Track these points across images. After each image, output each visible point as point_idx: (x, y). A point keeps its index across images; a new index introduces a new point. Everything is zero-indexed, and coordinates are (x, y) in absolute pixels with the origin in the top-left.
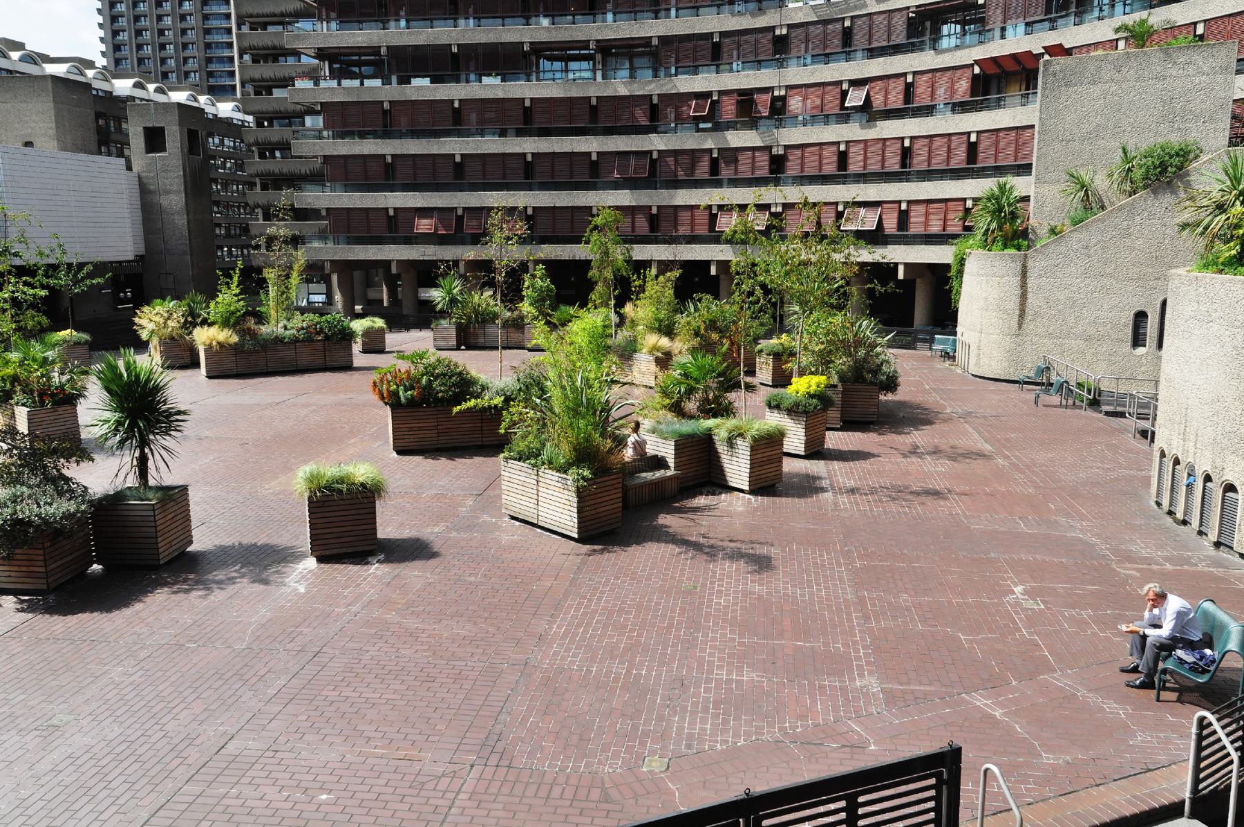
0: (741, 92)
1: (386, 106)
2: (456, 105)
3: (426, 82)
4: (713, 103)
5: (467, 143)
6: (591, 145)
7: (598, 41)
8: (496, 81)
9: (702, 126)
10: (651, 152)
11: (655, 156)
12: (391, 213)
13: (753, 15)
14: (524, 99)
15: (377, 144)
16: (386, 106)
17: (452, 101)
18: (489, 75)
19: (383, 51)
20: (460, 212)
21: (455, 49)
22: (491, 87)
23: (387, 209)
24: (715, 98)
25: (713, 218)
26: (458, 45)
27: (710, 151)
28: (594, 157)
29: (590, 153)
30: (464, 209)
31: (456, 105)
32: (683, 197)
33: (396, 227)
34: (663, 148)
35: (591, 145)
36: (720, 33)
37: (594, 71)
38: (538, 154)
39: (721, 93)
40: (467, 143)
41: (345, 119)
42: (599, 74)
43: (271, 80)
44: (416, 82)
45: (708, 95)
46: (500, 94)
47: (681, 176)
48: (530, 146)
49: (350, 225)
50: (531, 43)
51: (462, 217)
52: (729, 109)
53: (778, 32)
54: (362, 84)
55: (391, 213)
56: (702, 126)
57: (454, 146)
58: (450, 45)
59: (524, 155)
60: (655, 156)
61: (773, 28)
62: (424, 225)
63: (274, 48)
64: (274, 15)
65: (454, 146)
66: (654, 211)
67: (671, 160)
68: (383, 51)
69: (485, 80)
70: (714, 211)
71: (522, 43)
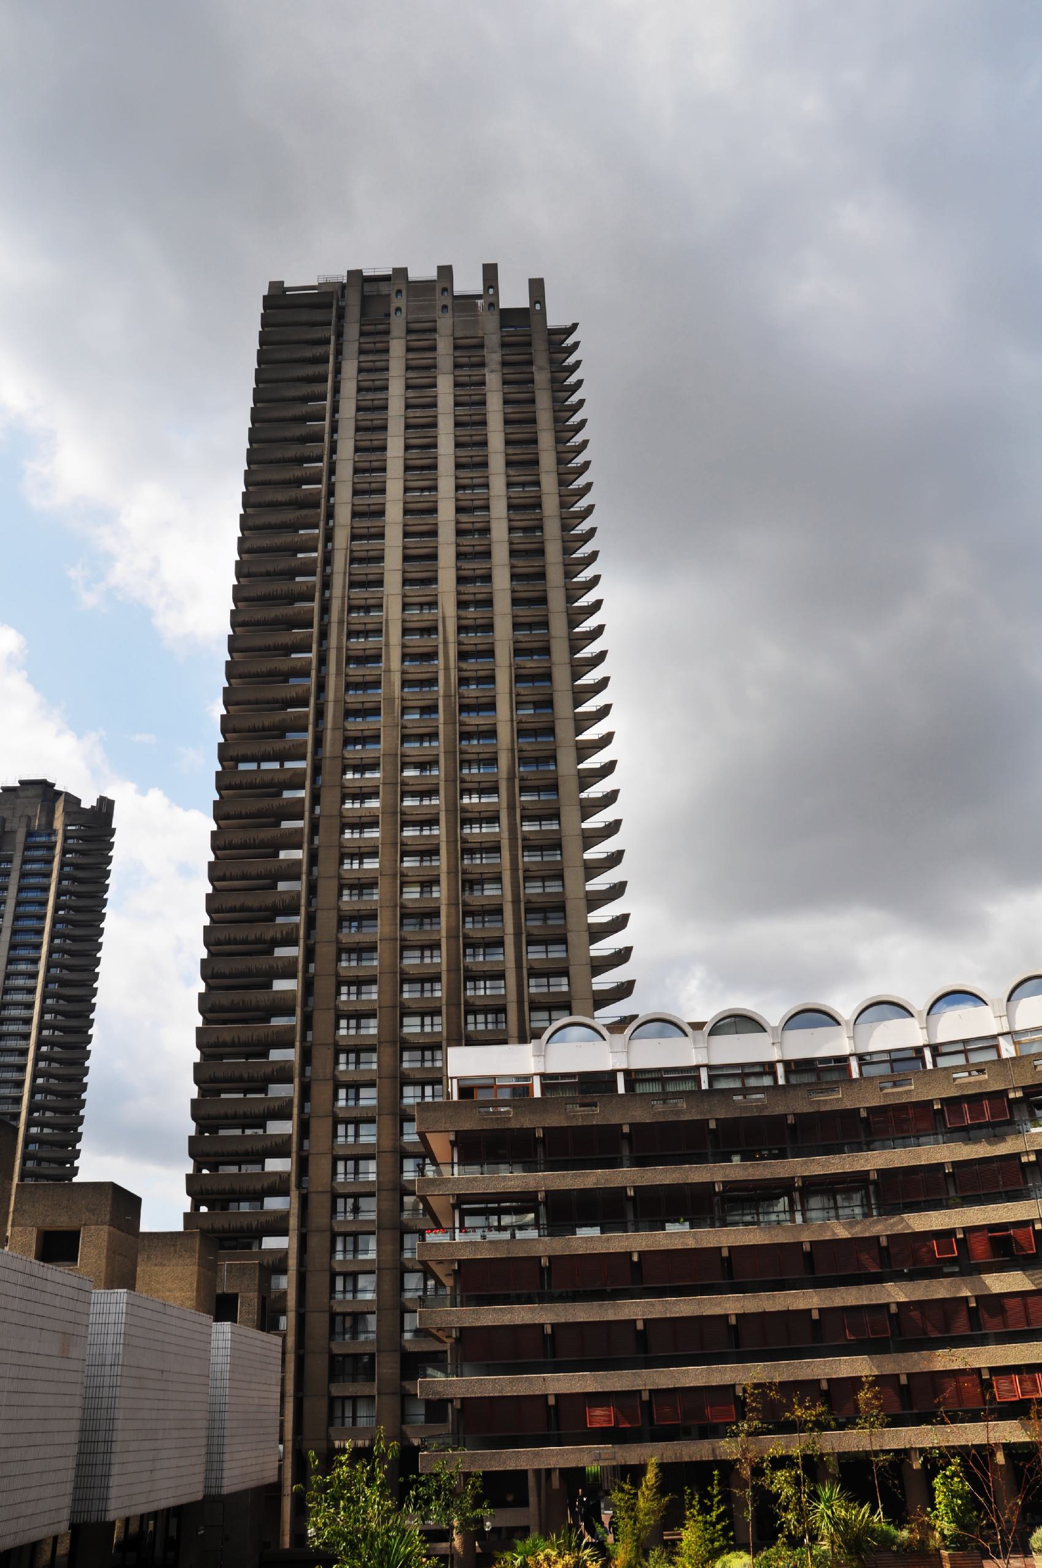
0: (992, 1228)
1: (544, 1262)
2: (635, 1258)
3: (595, 1232)
4: (958, 1241)
5: (652, 1305)
6: (809, 1300)
7: (802, 1177)
8: (685, 1227)
9: (946, 1270)
10: (887, 1306)
11: (893, 1309)
12: (552, 1401)
13: (990, 1143)
14: (720, 1248)
15: (532, 1310)
16: (544, 1262)
17: (630, 1254)
18: (677, 1221)
19: (541, 1196)
20: (645, 1397)
21: (631, 1193)
22: (678, 1235)
23: (546, 1396)
24: (960, 1236)
25: (987, 1385)
26: (636, 1188)
27: (966, 1298)
28: (815, 1315)
29: (810, 1311)
30: (650, 1391)
31: (635, 1258)
32: (946, 1360)
33: (559, 1420)
34: (903, 1299)
35: (809, 1300)
36: (953, 1163)
37: (792, 1211)
38: (744, 1314)
39: (966, 1230)
40: (652, 1305)
41: (479, 1280)
42: (799, 1218)
43: (224, 1231)
44: (583, 1232)
45: (951, 1232)
46: (691, 1244)
47: (935, 1335)
48: (731, 1305)
49: (486, 1423)
50: (723, 1182)
51: (650, 1402)
52: (980, 1248)
53: (1024, 1159)
54: (513, 1236)
55: (552, 1401)
56: (946, 1270)
57: (637, 1310)
58: (625, 1188)
59: (726, 1316)
60: (893, 1309)
61: (1018, 1156)
62: (599, 1417)
63: (233, 1191)
64: (237, 1154)
65: (637, 1310)
66: (904, 1380)
67: (915, 1314)
68: (541, 1196)
69: (671, 1228)
70: (986, 1376)
71: (713, 1183)
